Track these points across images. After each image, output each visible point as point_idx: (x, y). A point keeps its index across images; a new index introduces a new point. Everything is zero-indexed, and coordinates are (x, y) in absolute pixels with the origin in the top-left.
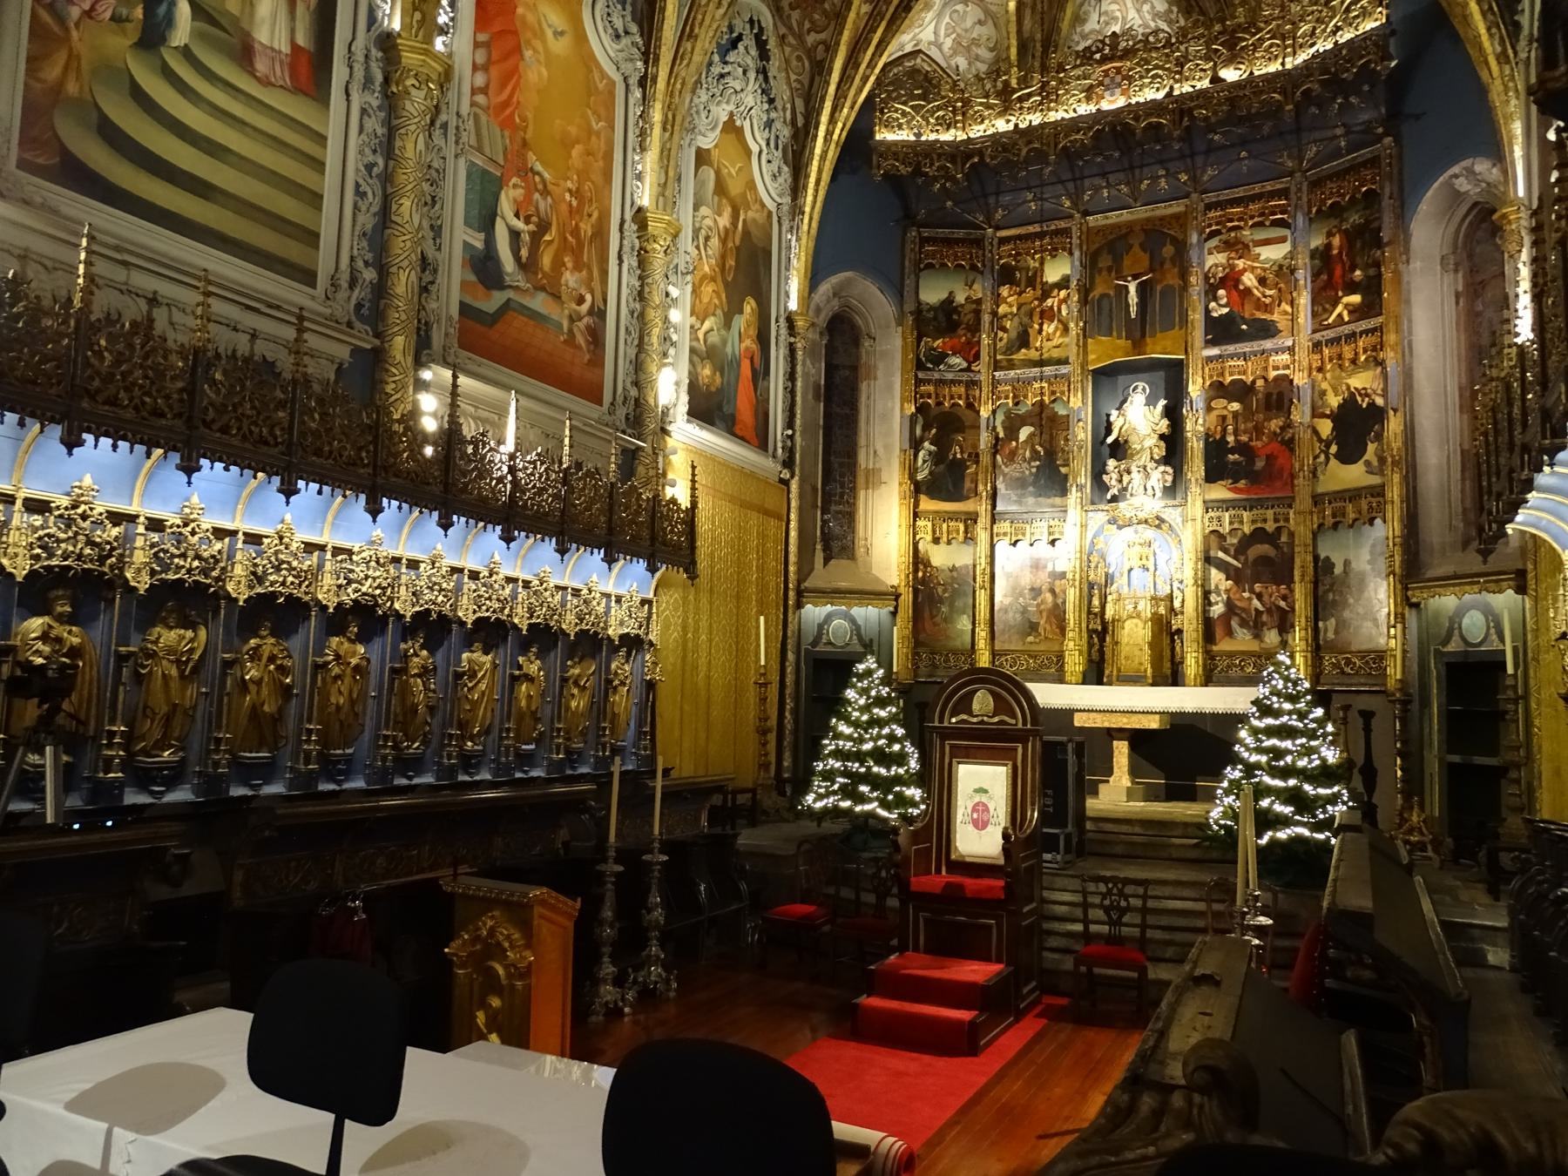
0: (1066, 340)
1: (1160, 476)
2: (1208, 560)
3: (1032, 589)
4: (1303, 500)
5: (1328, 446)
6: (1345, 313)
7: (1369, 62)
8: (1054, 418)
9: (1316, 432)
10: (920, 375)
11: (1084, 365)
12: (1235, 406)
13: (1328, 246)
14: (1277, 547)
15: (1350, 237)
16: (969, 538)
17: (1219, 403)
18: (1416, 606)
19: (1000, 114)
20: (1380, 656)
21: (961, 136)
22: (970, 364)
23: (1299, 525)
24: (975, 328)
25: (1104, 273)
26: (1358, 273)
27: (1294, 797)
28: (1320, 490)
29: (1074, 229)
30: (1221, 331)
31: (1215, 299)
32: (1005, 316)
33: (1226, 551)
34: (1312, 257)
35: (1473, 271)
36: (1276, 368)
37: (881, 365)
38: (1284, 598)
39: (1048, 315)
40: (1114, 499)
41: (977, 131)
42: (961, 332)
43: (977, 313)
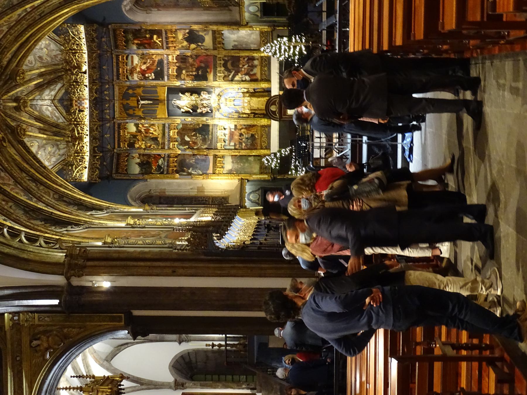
0: (157, 124)
1: (204, 95)
2: (232, 80)
3: (240, 136)
4: (215, 53)
5: (199, 45)
6: (159, 40)
7: (93, 30)
8: (183, 129)
9: (194, 49)
10: (165, 173)
11: (166, 118)
12: (184, 72)
13: (137, 44)
14: (228, 61)
15: (136, 37)
16: (223, 157)
17: (183, 76)
18: (247, 23)
19: (82, 141)
20: (262, 33)
21: (88, 154)
22: (161, 157)
23: (222, 54)
24: (149, 156)
25: (135, 112)
26: (147, 36)
27: (295, 47)
28: (212, 48)
29: (118, 122)
30: (159, 75)
31: (148, 77)
32: (146, 146)
33: (229, 75)
34: (139, 49)
35: (152, 6)
36: (173, 60)
37: (160, 187)
38: (244, 59)
39: (147, 131)
40: (212, 111)
41: (87, 149)
42: (150, 160)
43: (143, 155)
